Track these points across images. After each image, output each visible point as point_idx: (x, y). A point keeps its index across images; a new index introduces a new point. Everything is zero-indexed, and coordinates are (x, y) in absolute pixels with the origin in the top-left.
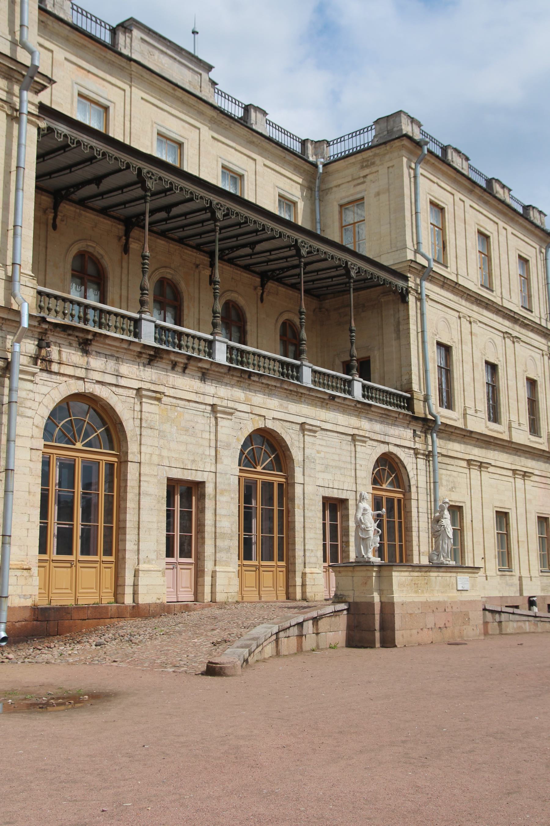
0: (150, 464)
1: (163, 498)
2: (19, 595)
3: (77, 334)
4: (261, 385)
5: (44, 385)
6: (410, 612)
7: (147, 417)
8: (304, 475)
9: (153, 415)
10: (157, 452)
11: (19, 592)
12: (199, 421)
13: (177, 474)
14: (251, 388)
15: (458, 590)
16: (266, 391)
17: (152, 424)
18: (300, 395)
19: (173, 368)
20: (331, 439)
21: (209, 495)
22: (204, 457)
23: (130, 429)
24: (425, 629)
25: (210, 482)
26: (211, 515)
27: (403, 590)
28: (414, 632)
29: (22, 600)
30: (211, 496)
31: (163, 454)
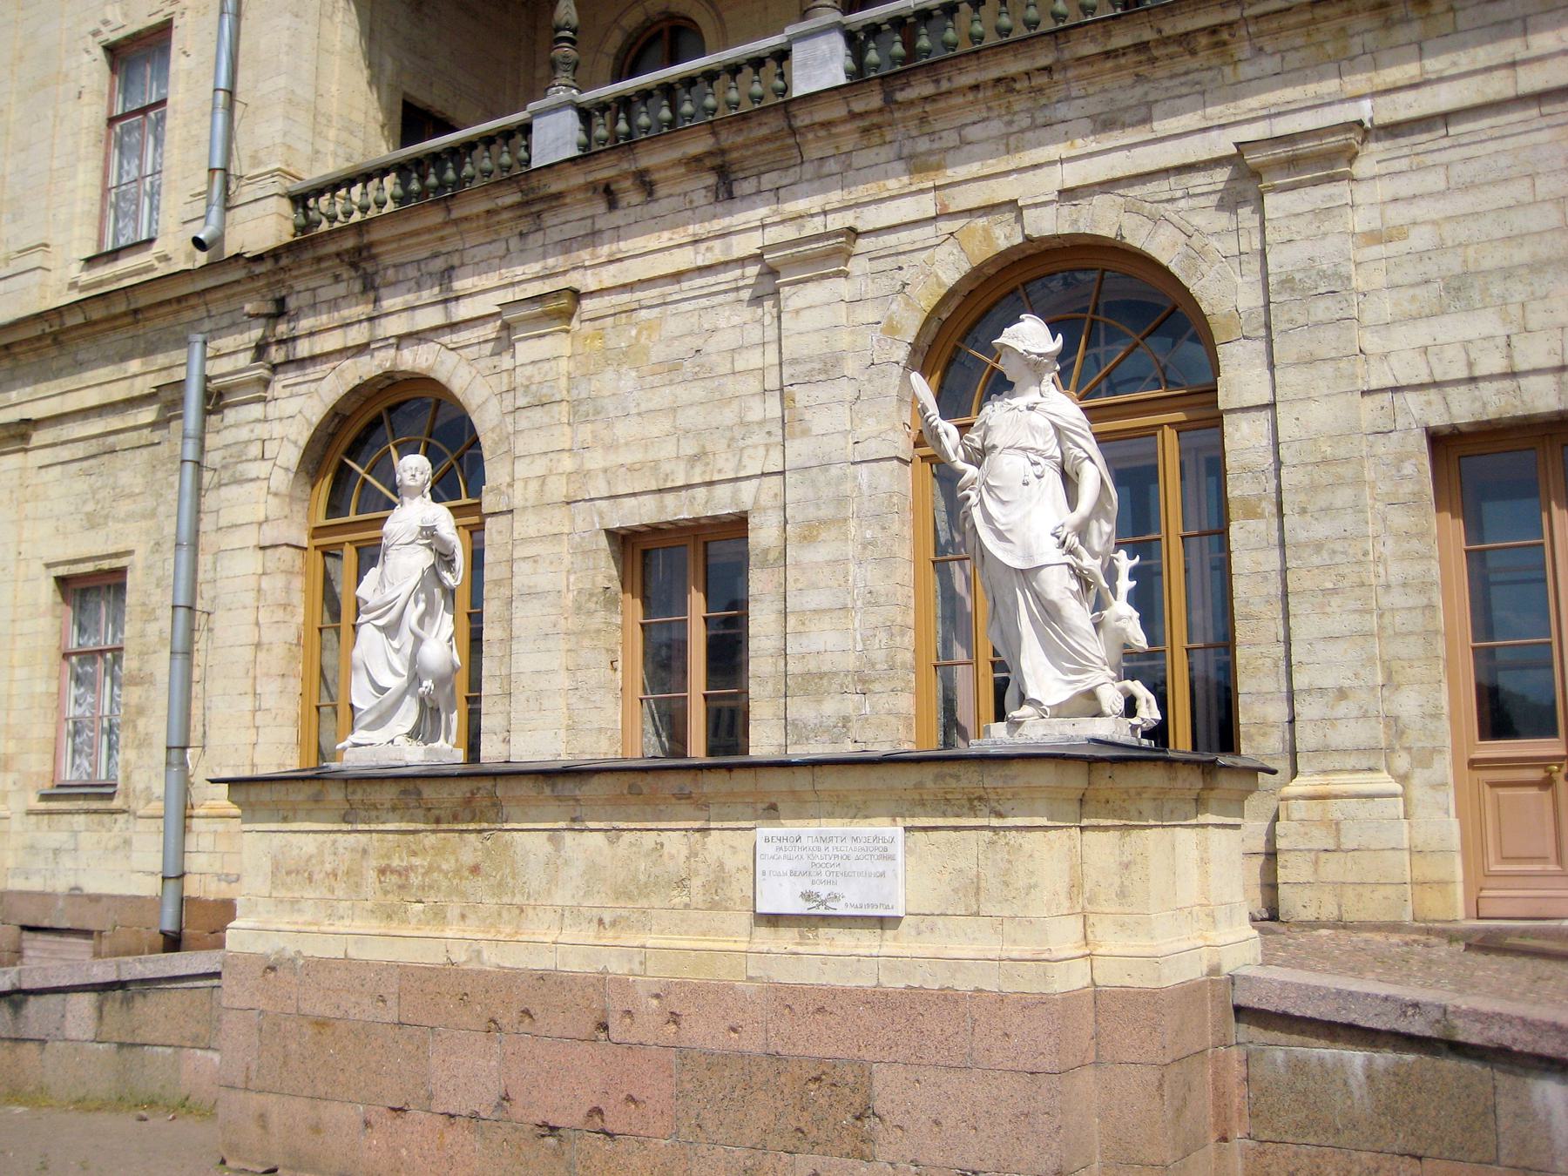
0: (541, 506)
1: (591, 595)
2: (218, 875)
3: (331, 248)
4: (971, 97)
5: (291, 396)
6: (323, 1009)
7: (529, 378)
8: (1272, 366)
9: (546, 366)
10: (567, 463)
11: (217, 867)
12: (722, 324)
13: (640, 513)
14: (938, 126)
15: (773, 920)
16: (1016, 108)
17: (545, 391)
18: (1203, 40)
19: (612, 205)
20: (1491, 147)
21: (766, 551)
22: (738, 433)
23: (489, 425)
24: (416, 1114)
25: (765, 509)
26: (773, 617)
27: (294, 902)
28: (342, 1115)
29: (224, 885)
30: (772, 556)
31: (589, 465)
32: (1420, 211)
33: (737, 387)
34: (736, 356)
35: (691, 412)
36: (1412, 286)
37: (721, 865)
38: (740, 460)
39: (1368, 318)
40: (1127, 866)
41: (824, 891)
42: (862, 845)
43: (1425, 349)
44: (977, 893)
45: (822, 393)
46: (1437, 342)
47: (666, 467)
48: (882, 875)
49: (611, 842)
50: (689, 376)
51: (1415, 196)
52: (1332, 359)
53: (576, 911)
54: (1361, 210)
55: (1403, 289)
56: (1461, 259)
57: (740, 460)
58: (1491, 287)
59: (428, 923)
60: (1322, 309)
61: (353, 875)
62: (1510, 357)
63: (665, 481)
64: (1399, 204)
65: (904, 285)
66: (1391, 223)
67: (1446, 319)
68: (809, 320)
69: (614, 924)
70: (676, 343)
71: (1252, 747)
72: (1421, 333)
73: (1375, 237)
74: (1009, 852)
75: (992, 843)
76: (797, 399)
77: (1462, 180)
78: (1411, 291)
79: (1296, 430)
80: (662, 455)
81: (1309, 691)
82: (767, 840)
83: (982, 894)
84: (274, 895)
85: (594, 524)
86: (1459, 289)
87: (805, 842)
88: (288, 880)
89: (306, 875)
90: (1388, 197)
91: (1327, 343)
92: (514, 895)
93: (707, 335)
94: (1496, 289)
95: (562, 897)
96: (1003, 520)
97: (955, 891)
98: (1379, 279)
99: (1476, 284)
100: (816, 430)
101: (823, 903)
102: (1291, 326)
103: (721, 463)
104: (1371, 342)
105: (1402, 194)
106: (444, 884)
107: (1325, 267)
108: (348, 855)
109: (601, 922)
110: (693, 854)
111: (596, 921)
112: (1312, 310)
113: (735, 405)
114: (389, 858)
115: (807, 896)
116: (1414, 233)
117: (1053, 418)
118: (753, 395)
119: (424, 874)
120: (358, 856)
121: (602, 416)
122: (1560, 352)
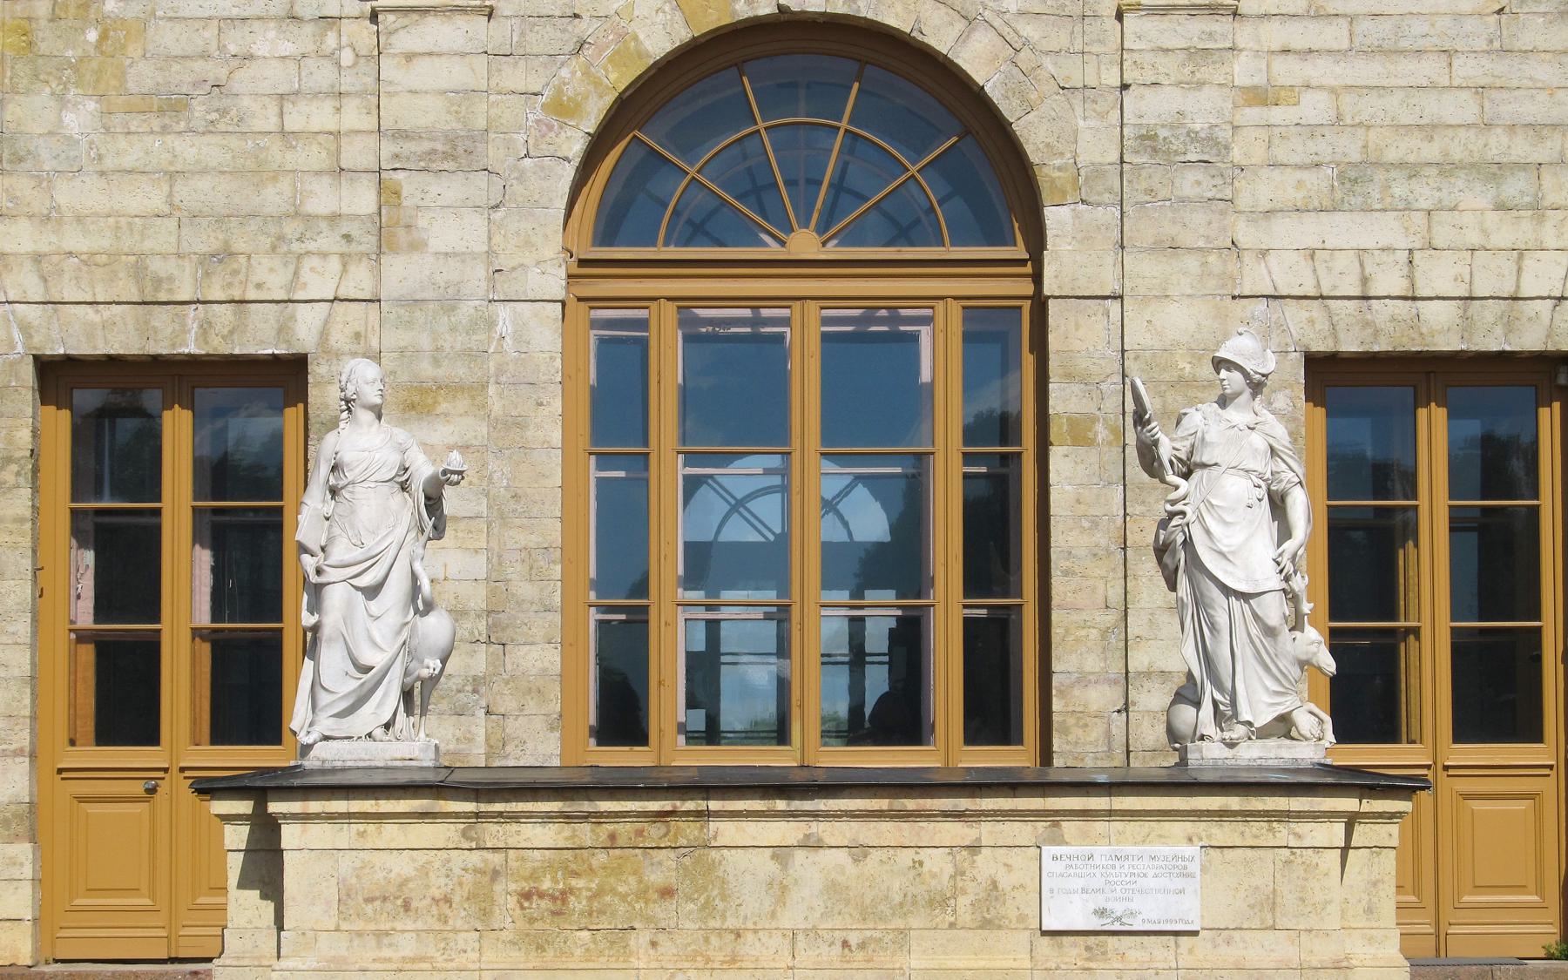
12: (261, 49)
22: (291, 228)
25: (338, 355)
32: (1320, 70)
33: (289, 156)
34: (288, 107)
35: (203, 184)
36: (1299, 167)
37: (994, 884)
38: (296, 273)
39: (1243, 202)
40: (1375, 884)
41: (1118, 908)
42: (1161, 863)
43: (1312, 254)
44: (1273, 909)
45: (449, 189)
46: (1327, 246)
47: (157, 266)
48: (1182, 891)
49: (856, 860)
50: (199, 125)
51: (1310, 51)
52: (1200, 249)
53: (813, 932)
54: (1243, 57)
55: (1289, 170)
56: (1360, 144)
57: (296, 273)
58: (1393, 184)
59: (601, 954)
60: (1190, 183)
61: (482, 904)
62: (1411, 278)
63: (157, 289)
64: (1290, 57)
65: (582, 44)
66: (1280, 81)
67: (1338, 216)
68: (426, 74)
69: (862, 946)
70: (176, 67)
71: (1068, 743)
72: (1309, 231)
73: (1259, 96)
74: (1305, 870)
75: (1287, 862)
76: (405, 193)
77: (1368, 42)
78: (1299, 175)
79: (1148, 336)
80: (148, 245)
81: (1148, 674)
82: (1055, 858)
83: (1278, 909)
84: (344, 926)
85: (12, 346)
86: (1356, 180)
87: (1097, 861)
88: (369, 909)
89: (399, 902)
90: (1276, 46)
91: (1197, 227)
92: (723, 917)
93: (235, 63)
94: (1399, 190)
95: (787, 920)
96: (1225, 541)
97: (1251, 907)
98: (1258, 154)
99: (1376, 178)
100: (436, 244)
101: (1119, 919)
102: (1148, 198)
103: (260, 274)
104: (1246, 235)
105: (1294, 45)
106: (622, 908)
107: (1197, 127)
108: (469, 878)
109: (845, 944)
110: (959, 873)
111: (839, 944)
112: (1177, 182)
113: (285, 185)
114: (536, 879)
115: (1101, 913)
116: (1308, 98)
117: (1272, 441)
118: (318, 173)
119: (590, 899)
120: (487, 878)
121: (28, 165)
122: (1467, 280)
